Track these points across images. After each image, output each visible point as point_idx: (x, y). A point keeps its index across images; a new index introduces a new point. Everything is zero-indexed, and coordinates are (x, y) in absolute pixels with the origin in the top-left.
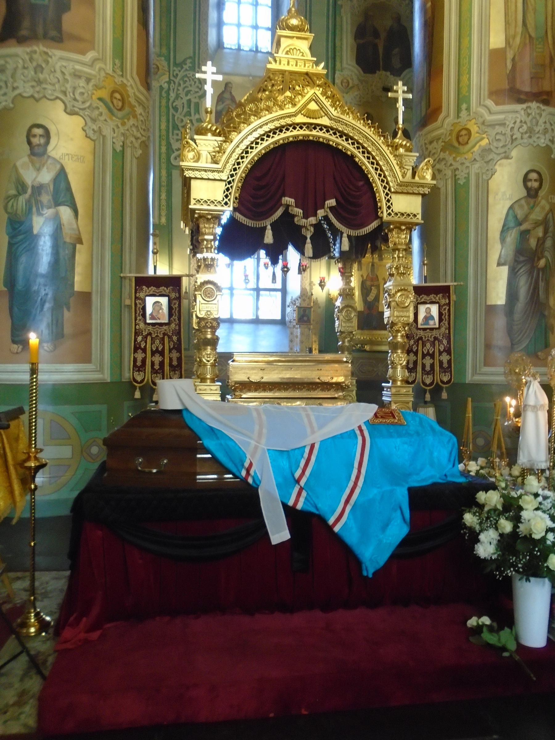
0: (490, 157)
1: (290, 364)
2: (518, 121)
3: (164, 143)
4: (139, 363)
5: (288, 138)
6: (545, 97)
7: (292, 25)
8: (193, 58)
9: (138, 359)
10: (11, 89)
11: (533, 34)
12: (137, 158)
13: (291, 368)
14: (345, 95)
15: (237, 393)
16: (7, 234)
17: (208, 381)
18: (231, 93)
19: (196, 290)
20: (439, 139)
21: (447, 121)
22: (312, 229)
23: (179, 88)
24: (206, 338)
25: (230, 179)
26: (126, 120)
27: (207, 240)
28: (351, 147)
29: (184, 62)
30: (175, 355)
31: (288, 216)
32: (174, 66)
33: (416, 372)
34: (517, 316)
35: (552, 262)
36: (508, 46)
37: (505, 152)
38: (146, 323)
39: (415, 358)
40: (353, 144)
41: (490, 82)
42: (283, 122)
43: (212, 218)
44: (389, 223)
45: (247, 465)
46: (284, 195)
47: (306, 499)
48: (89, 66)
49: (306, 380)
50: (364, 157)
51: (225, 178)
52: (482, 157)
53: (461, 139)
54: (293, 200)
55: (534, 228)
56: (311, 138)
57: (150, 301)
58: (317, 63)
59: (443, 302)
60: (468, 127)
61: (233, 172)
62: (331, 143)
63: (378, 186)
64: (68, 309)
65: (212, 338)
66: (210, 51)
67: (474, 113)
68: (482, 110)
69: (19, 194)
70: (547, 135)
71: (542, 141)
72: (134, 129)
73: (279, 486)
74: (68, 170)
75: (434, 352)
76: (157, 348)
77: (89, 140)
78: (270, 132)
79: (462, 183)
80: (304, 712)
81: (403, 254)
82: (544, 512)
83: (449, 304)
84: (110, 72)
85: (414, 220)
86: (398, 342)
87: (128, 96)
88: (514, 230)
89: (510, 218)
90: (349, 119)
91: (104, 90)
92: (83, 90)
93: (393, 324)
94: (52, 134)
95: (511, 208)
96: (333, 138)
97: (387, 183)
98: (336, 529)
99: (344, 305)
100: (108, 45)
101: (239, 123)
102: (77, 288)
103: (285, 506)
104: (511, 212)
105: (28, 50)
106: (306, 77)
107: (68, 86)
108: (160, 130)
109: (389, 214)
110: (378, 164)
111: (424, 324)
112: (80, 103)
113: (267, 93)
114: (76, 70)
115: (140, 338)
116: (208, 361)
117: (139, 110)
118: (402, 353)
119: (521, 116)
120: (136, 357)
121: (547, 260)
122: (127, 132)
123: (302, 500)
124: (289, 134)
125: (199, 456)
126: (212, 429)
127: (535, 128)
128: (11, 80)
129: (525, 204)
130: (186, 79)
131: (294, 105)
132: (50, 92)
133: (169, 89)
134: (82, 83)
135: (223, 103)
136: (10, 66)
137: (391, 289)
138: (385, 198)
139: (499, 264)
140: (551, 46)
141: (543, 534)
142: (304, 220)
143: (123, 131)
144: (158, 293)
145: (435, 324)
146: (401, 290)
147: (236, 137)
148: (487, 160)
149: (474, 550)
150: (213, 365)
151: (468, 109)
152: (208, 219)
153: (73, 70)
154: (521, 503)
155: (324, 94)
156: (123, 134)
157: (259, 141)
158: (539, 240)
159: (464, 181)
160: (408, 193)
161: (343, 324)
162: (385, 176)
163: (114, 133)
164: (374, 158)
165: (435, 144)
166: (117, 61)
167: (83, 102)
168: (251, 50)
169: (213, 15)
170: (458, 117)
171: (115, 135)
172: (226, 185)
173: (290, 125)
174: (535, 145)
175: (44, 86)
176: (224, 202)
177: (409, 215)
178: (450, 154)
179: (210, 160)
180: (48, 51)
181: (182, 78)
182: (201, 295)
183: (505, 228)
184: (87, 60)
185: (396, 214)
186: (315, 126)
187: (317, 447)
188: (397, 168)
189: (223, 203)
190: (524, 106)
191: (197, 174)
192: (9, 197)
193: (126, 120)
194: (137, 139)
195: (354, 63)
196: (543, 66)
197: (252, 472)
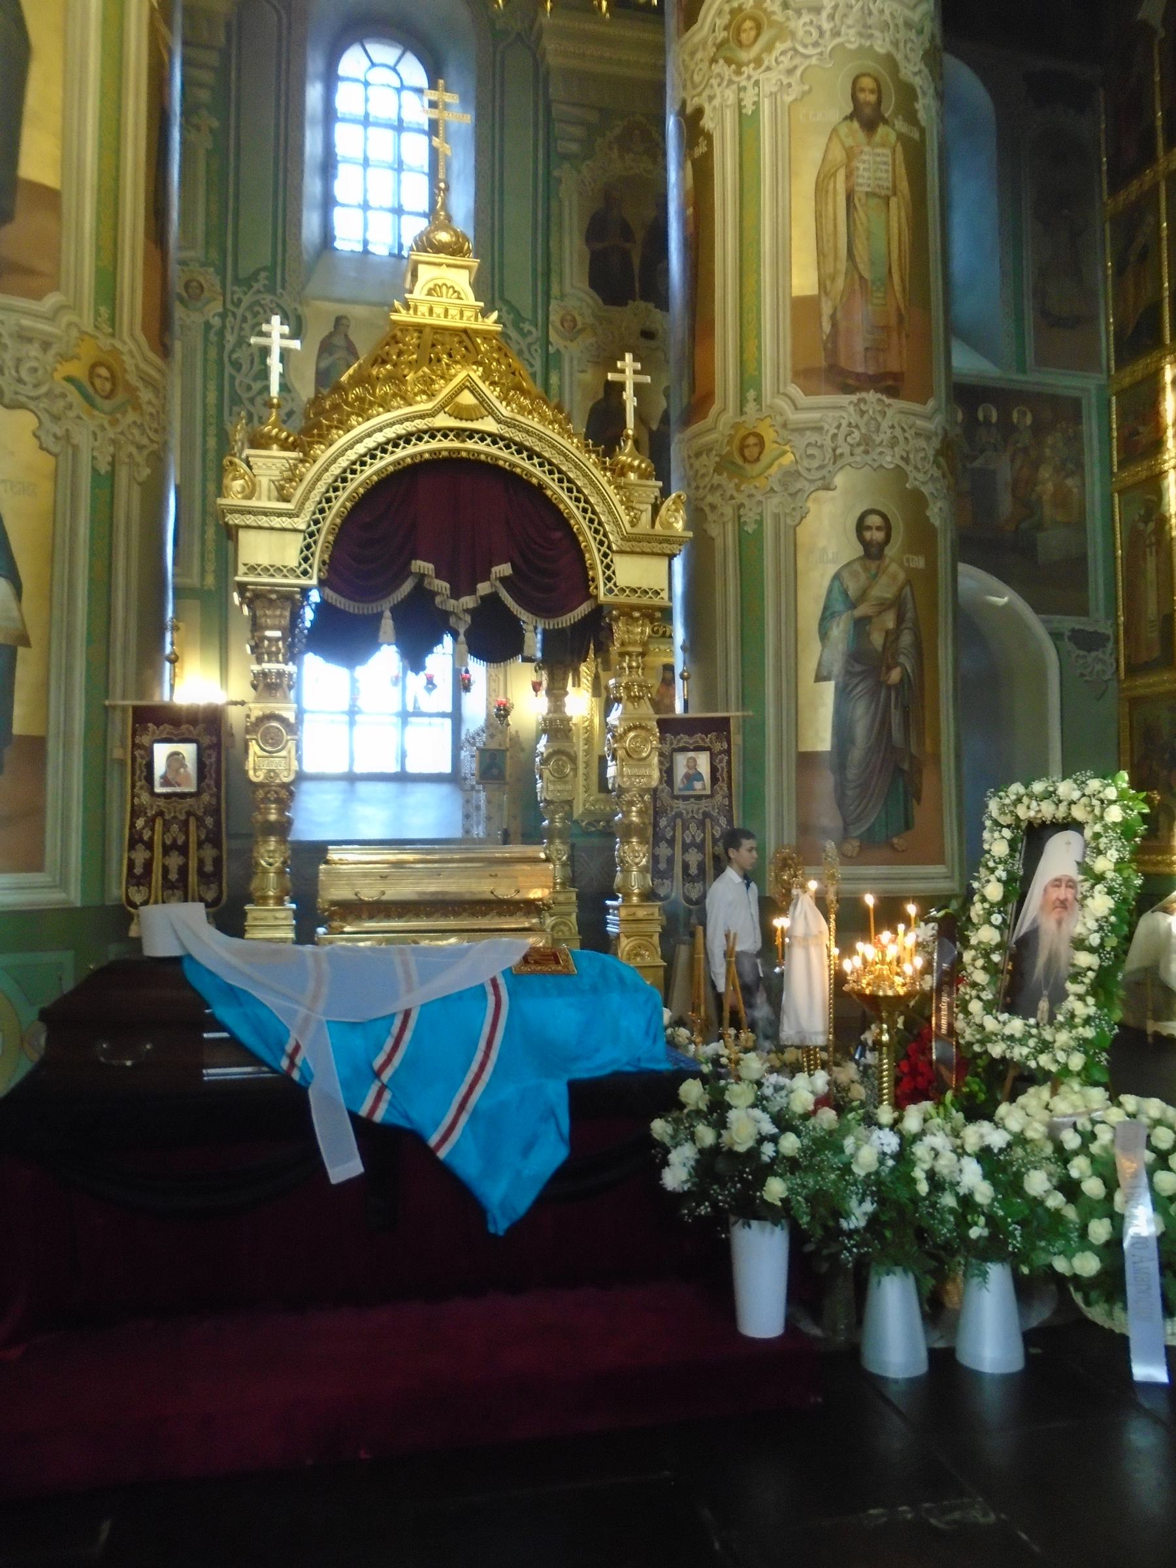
0: (798, 486)
1: (436, 865)
2: (844, 423)
3: (212, 430)
4: (138, 870)
5: (421, 454)
6: (890, 383)
7: (440, 241)
8: (272, 269)
9: (137, 861)
11: (866, 275)
12: (140, 484)
13: (438, 874)
14: (568, 343)
15: (335, 924)
17: (271, 902)
18: (346, 336)
19: (247, 731)
20: (711, 450)
21: (723, 419)
22: (468, 618)
23: (245, 326)
24: (267, 821)
25: (313, 528)
26: (119, 416)
27: (269, 639)
28: (537, 471)
29: (255, 276)
30: (209, 853)
31: (422, 595)
32: (233, 284)
33: (672, 877)
34: (852, 773)
35: (913, 671)
36: (823, 294)
37: (824, 478)
38: (152, 793)
39: (668, 852)
40: (541, 465)
41: (794, 353)
42: (410, 426)
43: (279, 598)
44: (614, 606)
45: (289, 1048)
46: (416, 559)
47: (391, 1104)
49: (467, 897)
50: (562, 488)
51: (303, 527)
52: (784, 485)
53: (747, 452)
54: (431, 566)
55: (880, 613)
56: (464, 454)
57: (161, 752)
58: (485, 313)
59: (718, 747)
60: (758, 430)
61: (318, 516)
62: (501, 463)
63: (588, 540)
65: (277, 822)
66: (305, 257)
67: (768, 406)
68: (782, 403)
70: (896, 449)
71: (889, 459)
72: (135, 431)
73: (345, 1085)
75: (703, 840)
76: (175, 840)
77: (44, 453)
78: (387, 443)
79: (750, 531)
80: (363, 1455)
81: (637, 661)
82: (764, 1109)
83: (728, 752)
84: (90, 329)
85: (656, 601)
86: (632, 823)
87: (125, 370)
88: (844, 617)
89: (836, 594)
90: (533, 422)
91: (76, 361)
92: (35, 364)
93: (621, 791)
95: (837, 577)
96: (505, 454)
97: (605, 535)
98: (442, 1154)
99: (551, 750)
100: (86, 279)
101: (329, 428)
102: (18, 728)
103: (354, 1117)
104: (837, 583)
106: (464, 337)
108: (205, 405)
109: (611, 591)
110: (587, 501)
111: (686, 789)
112: (30, 387)
113: (389, 367)
114: (22, 328)
115: (140, 823)
116: (270, 864)
117: (145, 395)
118: (640, 843)
119: (850, 414)
120: (133, 857)
121: (904, 669)
122: (121, 437)
123: (383, 1107)
124: (422, 447)
125: (205, 1035)
126: (231, 988)
127: (874, 437)
129: (861, 570)
130: (257, 308)
131: (431, 395)
133: (224, 327)
134: (34, 350)
135: (331, 354)
137: (616, 727)
138: (602, 562)
139: (819, 678)
140: (899, 295)
141: (751, 1143)
142: (453, 602)
143: (113, 436)
145: (704, 789)
146: (635, 728)
147: (323, 454)
148: (792, 490)
149: (661, 1179)
150: (280, 873)
151: (758, 400)
152: (271, 600)
153: (17, 328)
154: (727, 1098)
155: (484, 378)
156: (114, 442)
157: (367, 459)
158: (887, 633)
159: (755, 526)
160: (643, 553)
161: (551, 787)
162: (600, 523)
163: (96, 440)
164: (579, 491)
165: (704, 459)
166: (103, 310)
167: (36, 386)
168: (391, 255)
169: (312, 186)
170: (742, 413)
171: (97, 444)
172: (305, 539)
173: (425, 432)
174: (875, 465)
176: (302, 568)
177: (646, 592)
178: (730, 478)
179: (275, 493)
181: (250, 308)
182: (256, 740)
183: (828, 613)
185: (623, 590)
186: (471, 434)
187: (414, 1016)
188: (621, 509)
189: (298, 572)
190: (854, 398)
191: (250, 520)
193: (119, 416)
194: (140, 448)
195: (585, 285)
196: (886, 328)
197: (298, 1060)
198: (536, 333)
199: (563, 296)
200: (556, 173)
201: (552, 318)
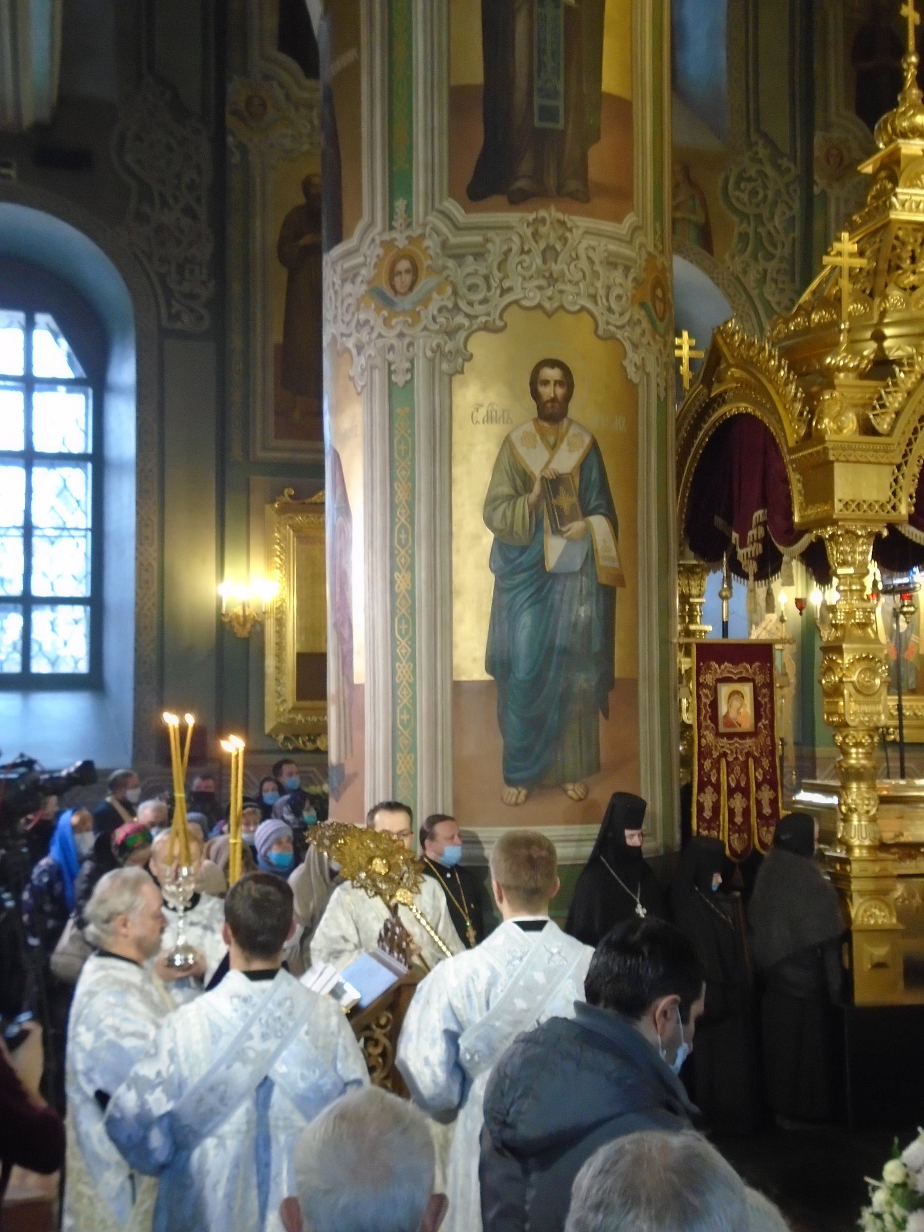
4: (707, 814)
10: (498, 292)
57: (724, 690)
64: (606, 716)
69: (518, 494)
105: (531, 217)
107: (599, 284)
112: (617, 315)
114: (611, 254)
115: (707, 764)
128: (497, 275)
132: (570, 298)
136: (495, 249)
144: (735, 674)
153: (605, 254)
166: (658, 225)
167: (621, 314)
175: (560, 286)
176: (892, 504)
180: (566, 218)
189: (889, 507)
195: (852, 115)
198: (795, 171)
201: (817, 153)
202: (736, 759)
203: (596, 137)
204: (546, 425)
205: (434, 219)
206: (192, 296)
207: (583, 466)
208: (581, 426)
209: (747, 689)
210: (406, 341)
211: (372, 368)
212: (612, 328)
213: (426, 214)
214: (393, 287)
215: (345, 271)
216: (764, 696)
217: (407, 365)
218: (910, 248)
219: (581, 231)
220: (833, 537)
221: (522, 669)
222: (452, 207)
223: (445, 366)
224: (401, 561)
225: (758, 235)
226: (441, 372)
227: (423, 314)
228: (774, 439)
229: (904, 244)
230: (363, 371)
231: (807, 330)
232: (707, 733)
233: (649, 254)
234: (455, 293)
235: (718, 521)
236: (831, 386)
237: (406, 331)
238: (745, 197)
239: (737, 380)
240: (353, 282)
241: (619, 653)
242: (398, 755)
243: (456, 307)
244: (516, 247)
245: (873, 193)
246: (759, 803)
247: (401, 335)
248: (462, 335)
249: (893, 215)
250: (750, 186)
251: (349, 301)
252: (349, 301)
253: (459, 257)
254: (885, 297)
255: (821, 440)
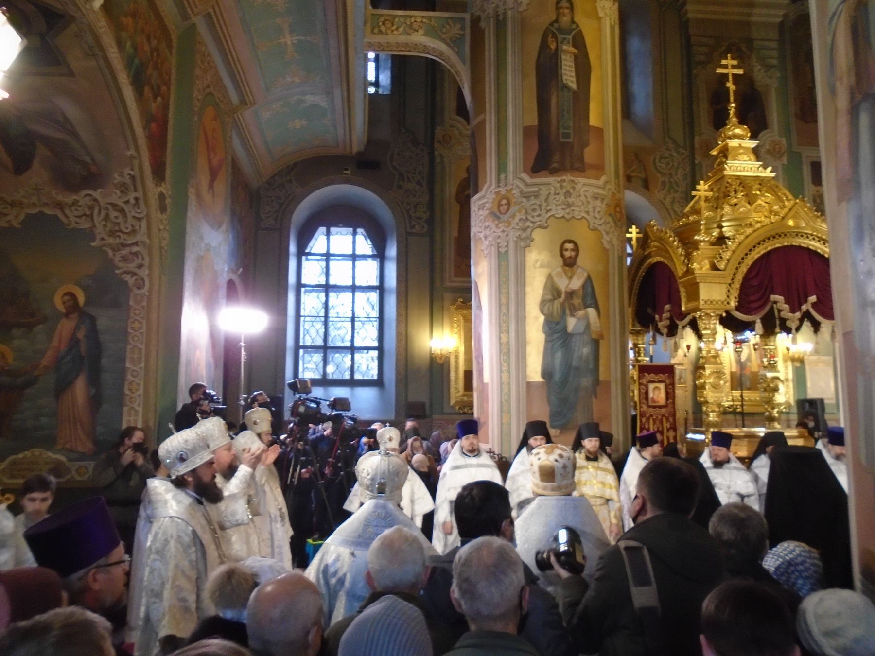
10: (545, 211)
16: (544, 333)
48: (602, 188)
58: (765, 168)
64: (596, 398)
74: (593, 278)
76: (658, 428)
94: (581, 249)
105: (559, 179)
107: (590, 206)
115: (644, 420)
128: (545, 204)
132: (577, 213)
136: (544, 193)
142: (791, 315)
167: (601, 219)
175: (573, 208)
184: (601, 184)
189: (726, 303)
192: (546, 301)
199: (701, 134)
200: (695, 72)
201: (696, 146)
202: (657, 417)
203: (587, 145)
204: (567, 268)
205: (517, 182)
206: (419, 218)
207: (584, 286)
208: (583, 268)
209: (662, 386)
210: (506, 233)
211: (492, 245)
212: (596, 225)
213: (513, 180)
214: (499, 211)
215: (480, 205)
216: (670, 389)
217: (506, 244)
218: (734, 187)
219: (581, 184)
220: (700, 316)
221: (557, 377)
222: (525, 176)
223: (522, 244)
224: (504, 328)
225: (670, 182)
226: (521, 246)
227: (512, 222)
228: (673, 273)
229: (731, 185)
230: (487, 247)
231: (688, 224)
232: (643, 406)
233: (613, 192)
234: (526, 212)
235: (650, 310)
236: (697, 249)
237: (505, 230)
238: (664, 166)
239: (656, 247)
240: (483, 210)
241: (601, 369)
242: (503, 414)
243: (527, 219)
244: (552, 192)
245: (717, 163)
246: (668, 438)
247: (503, 231)
248: (529, 230)
249: (725, 173)
250: (665, 161)
251: (481, 218)
252: (481, 218)
253: (527, 197)
254: (723, 209)
255: (693, 273)
